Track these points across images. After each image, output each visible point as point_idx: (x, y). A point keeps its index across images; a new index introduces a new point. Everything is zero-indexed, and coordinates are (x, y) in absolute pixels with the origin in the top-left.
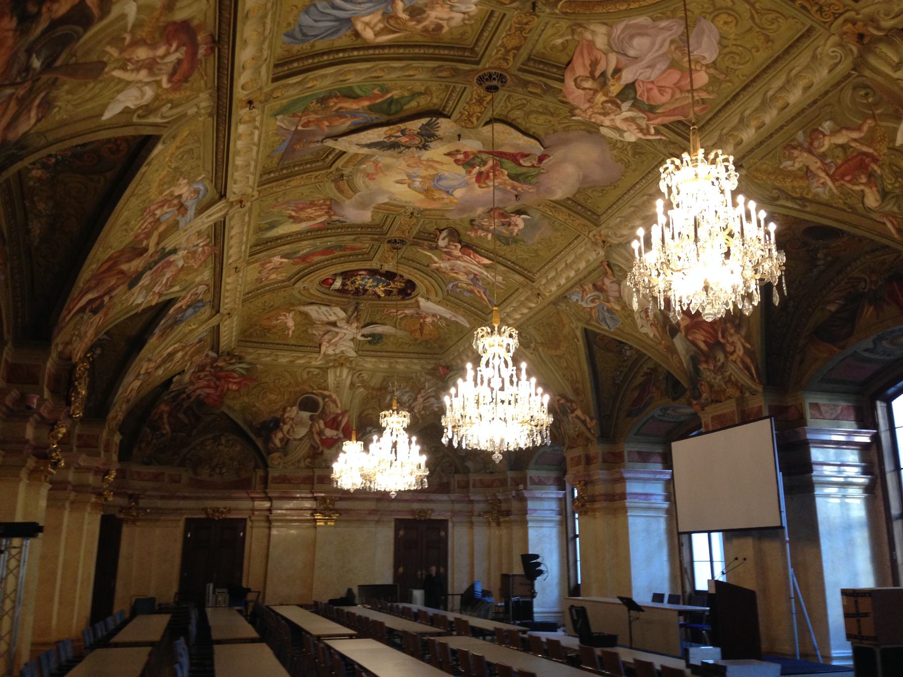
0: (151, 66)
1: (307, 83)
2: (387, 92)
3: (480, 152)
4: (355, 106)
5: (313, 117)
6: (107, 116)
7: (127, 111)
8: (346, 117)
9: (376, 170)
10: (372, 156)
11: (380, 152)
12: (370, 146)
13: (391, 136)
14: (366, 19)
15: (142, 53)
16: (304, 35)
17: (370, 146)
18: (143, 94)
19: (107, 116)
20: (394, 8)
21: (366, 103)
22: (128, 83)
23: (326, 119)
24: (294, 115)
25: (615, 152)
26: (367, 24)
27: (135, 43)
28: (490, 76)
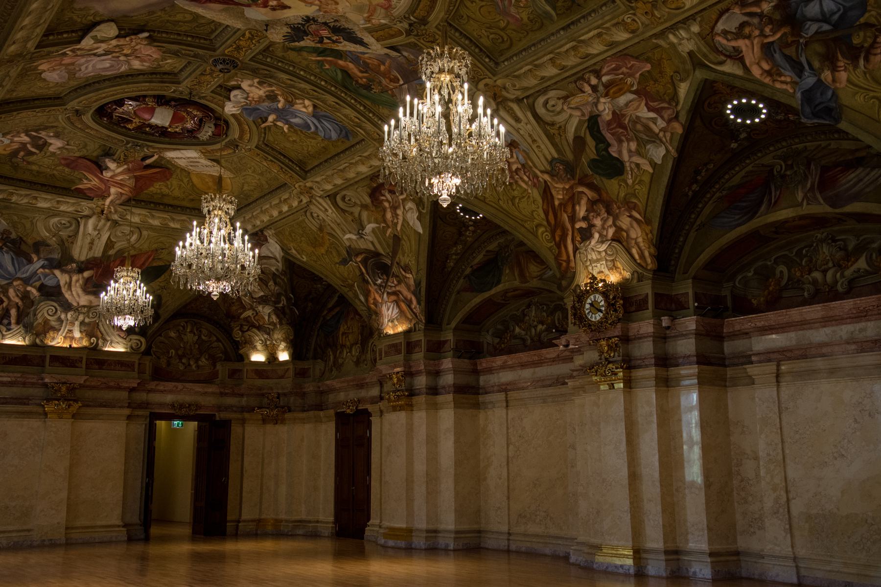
0: (394, 208)
1: (357, 123)
2: (319, 61)
3: (249, 6)
4: (351, 66)
5: (384, 82)
6: (421, 231)
7: (419, 218)
8: (364, 62)
9: (375, 10)
10: (366, 29)
11: (356, 29)
12: (360, 42)
13: (334, 42)
14: (304, 110)
15: (389, 215)
16: (341, 131)
17: (360, 42)
18: (410, 209)
19: (421, 231)
20: (285, 105)
21: (341, 62)
22: (404, 220)
23: (378, 72)
24: (393, 95)
25: (92, 12)
26: (305, 107)
27: (385, 221)
28: (224, 61)
